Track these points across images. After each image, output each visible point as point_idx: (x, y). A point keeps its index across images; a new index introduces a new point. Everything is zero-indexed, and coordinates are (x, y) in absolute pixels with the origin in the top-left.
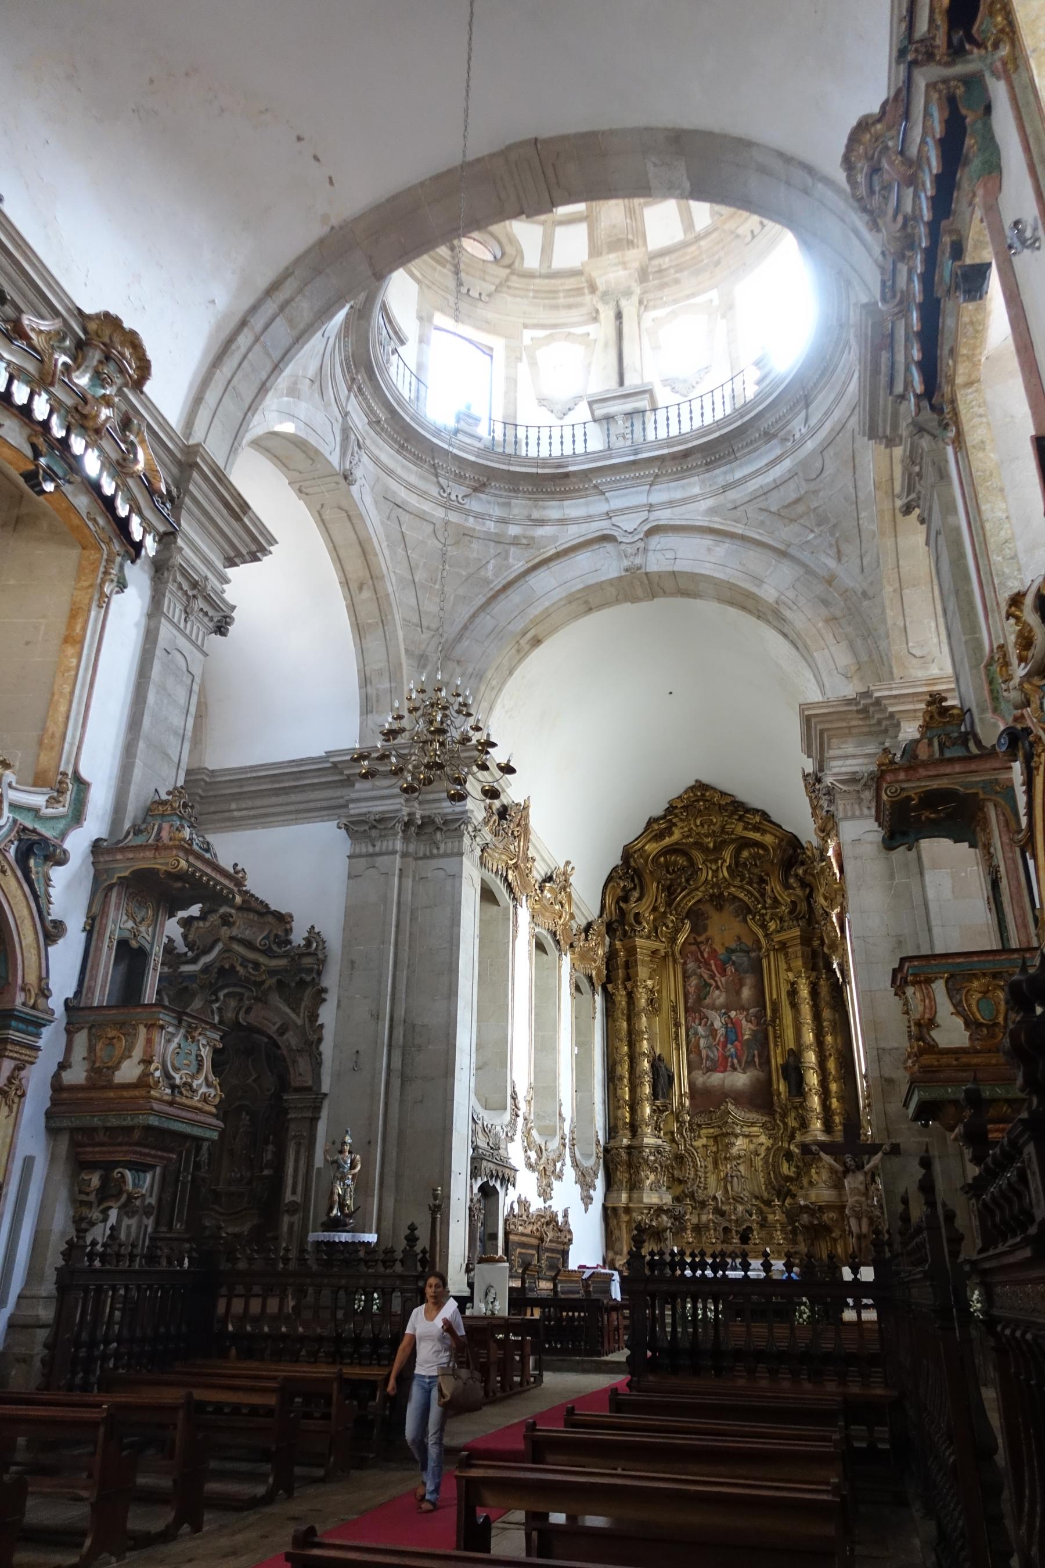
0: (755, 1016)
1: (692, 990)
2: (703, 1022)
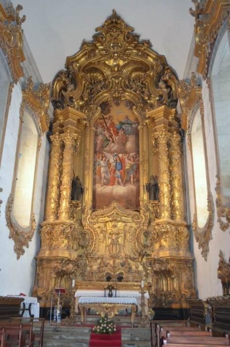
0: (133, 157)
1: (99, 142)
2: (104, 159)
